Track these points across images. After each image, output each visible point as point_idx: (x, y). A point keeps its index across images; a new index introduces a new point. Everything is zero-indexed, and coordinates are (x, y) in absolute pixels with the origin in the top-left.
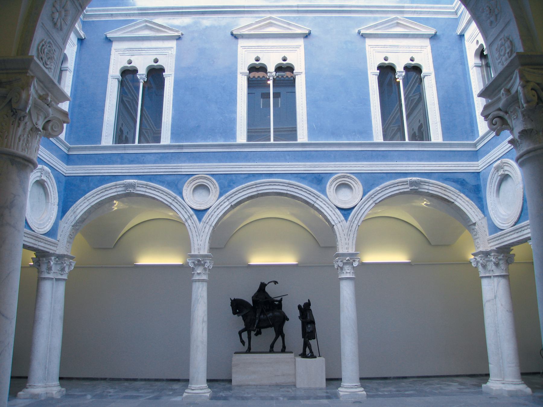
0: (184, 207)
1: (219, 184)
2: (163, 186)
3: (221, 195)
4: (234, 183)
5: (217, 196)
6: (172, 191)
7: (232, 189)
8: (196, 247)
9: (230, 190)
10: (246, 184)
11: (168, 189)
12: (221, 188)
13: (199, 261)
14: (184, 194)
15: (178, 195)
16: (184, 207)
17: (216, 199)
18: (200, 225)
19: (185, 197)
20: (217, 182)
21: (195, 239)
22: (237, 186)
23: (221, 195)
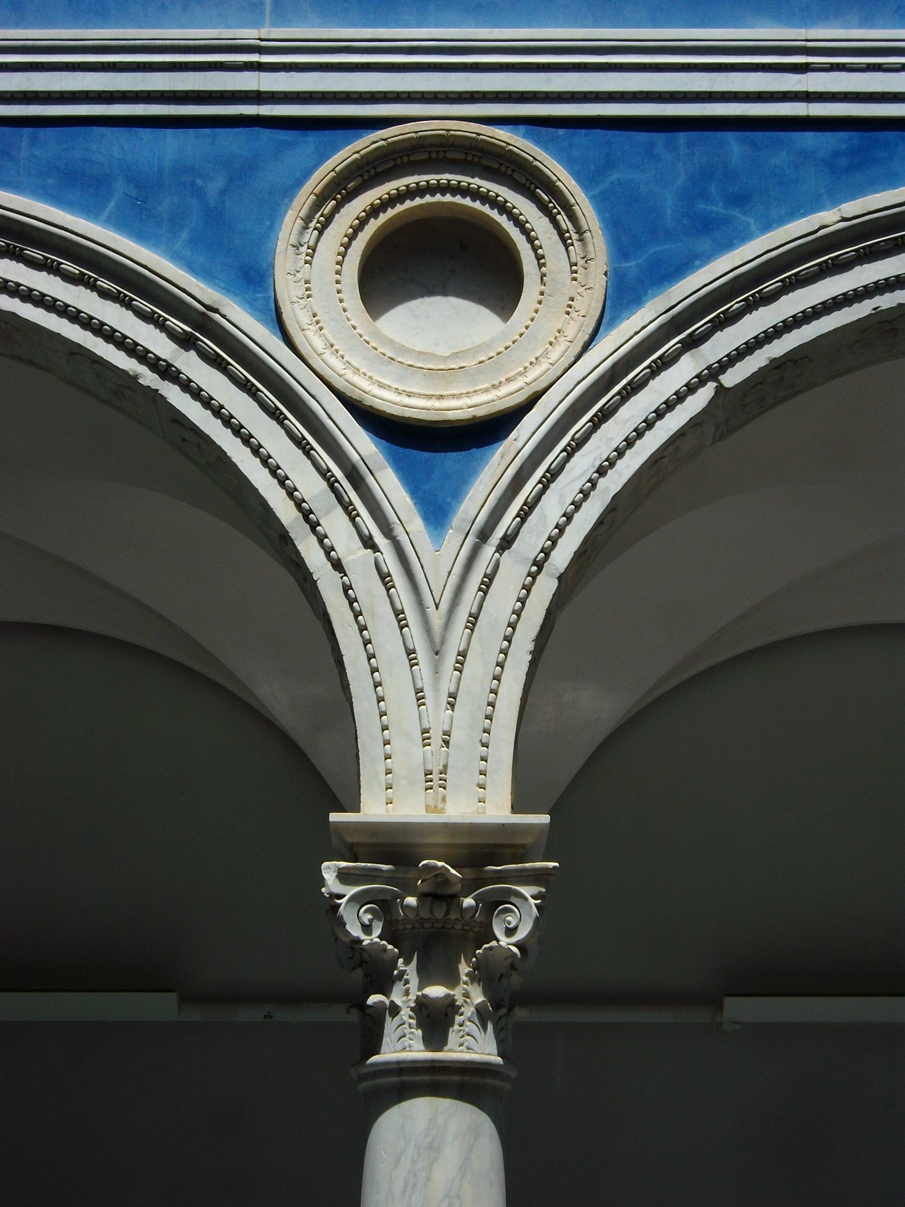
0: (285, 402)
1: (601, 202)
2: (90, 211)
3: (621, 297)
4: (740, 200)
5: (590, 303)
6: (176, 257)
7: (729, 245)
8: (410, 755)
9: (706, 258)
10: (854, 207)
11: (140, 237)
12: (621, 249)
13: (440, 895)
14: (287, 289)
15: (228, 290)
16: (285, 402)
17: (577, 329)
18: (439, 557)
19: (296, 316)
20: (586, 181)
21: (397, 681)
22: (767, 227)
23: (621, 297)
